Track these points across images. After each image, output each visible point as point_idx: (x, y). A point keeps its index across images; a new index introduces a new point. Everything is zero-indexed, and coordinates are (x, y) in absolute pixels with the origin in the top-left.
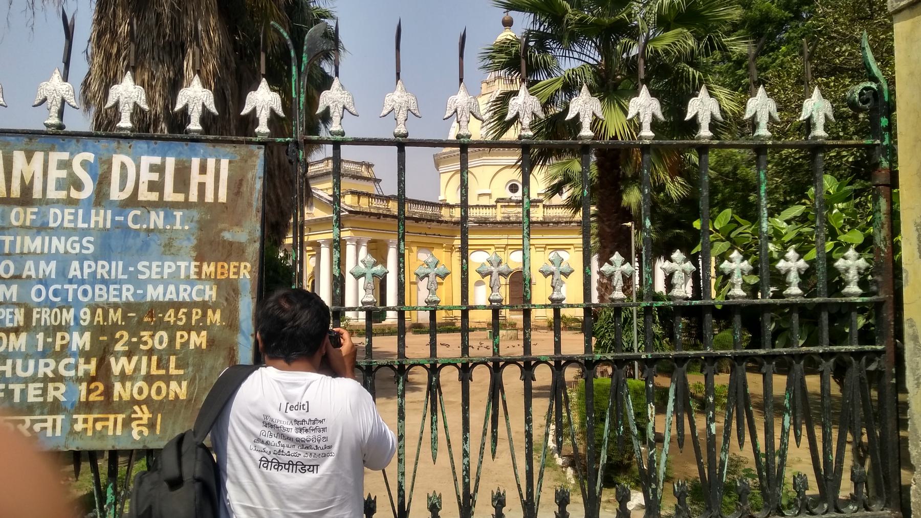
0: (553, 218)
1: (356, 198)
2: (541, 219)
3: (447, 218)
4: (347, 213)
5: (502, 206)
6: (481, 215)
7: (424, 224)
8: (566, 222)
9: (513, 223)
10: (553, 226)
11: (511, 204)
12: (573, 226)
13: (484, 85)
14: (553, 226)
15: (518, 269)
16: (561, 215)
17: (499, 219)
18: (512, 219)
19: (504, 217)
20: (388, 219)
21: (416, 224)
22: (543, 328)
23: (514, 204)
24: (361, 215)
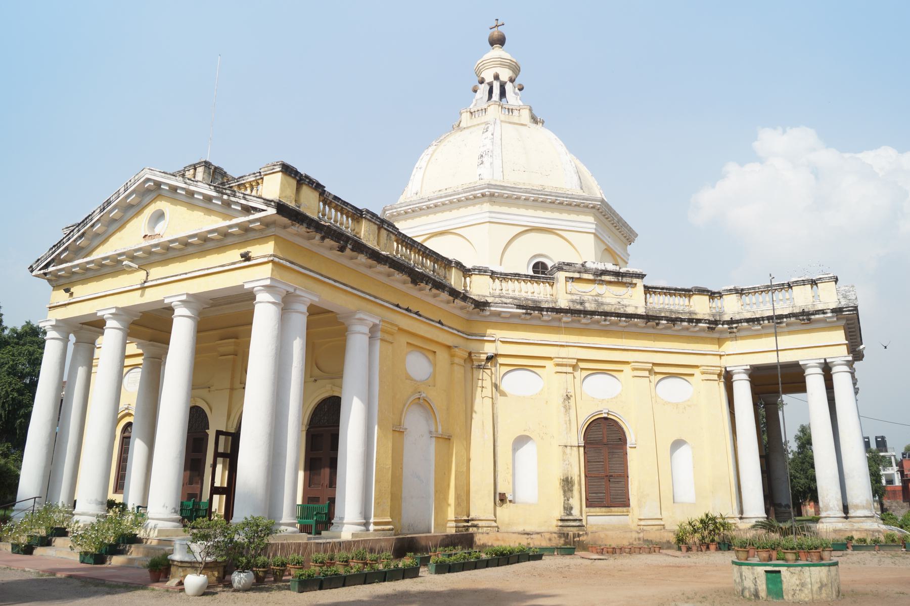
0: (660, 311)
1: (294, 183)
2: (641, 311)
3: (460, 289)
4: (272, 211)
5: (568, 279)
6: (524, 295)
7: (425, 293)
8: (690, 321)
9: (593, 313)
10: (666, 328)
11: (585, 276)
12: (702, 330)
13: (465, 116)
14: (666, 328)
15: (600, 412)
16: (677, 307)
17: (563, 304)
18: (590, 307)
19: (573, 301)
20: (362, 258)
21: (410, 289)
22: (668, 545)
23: (591, 277)
24: (302, 229)
